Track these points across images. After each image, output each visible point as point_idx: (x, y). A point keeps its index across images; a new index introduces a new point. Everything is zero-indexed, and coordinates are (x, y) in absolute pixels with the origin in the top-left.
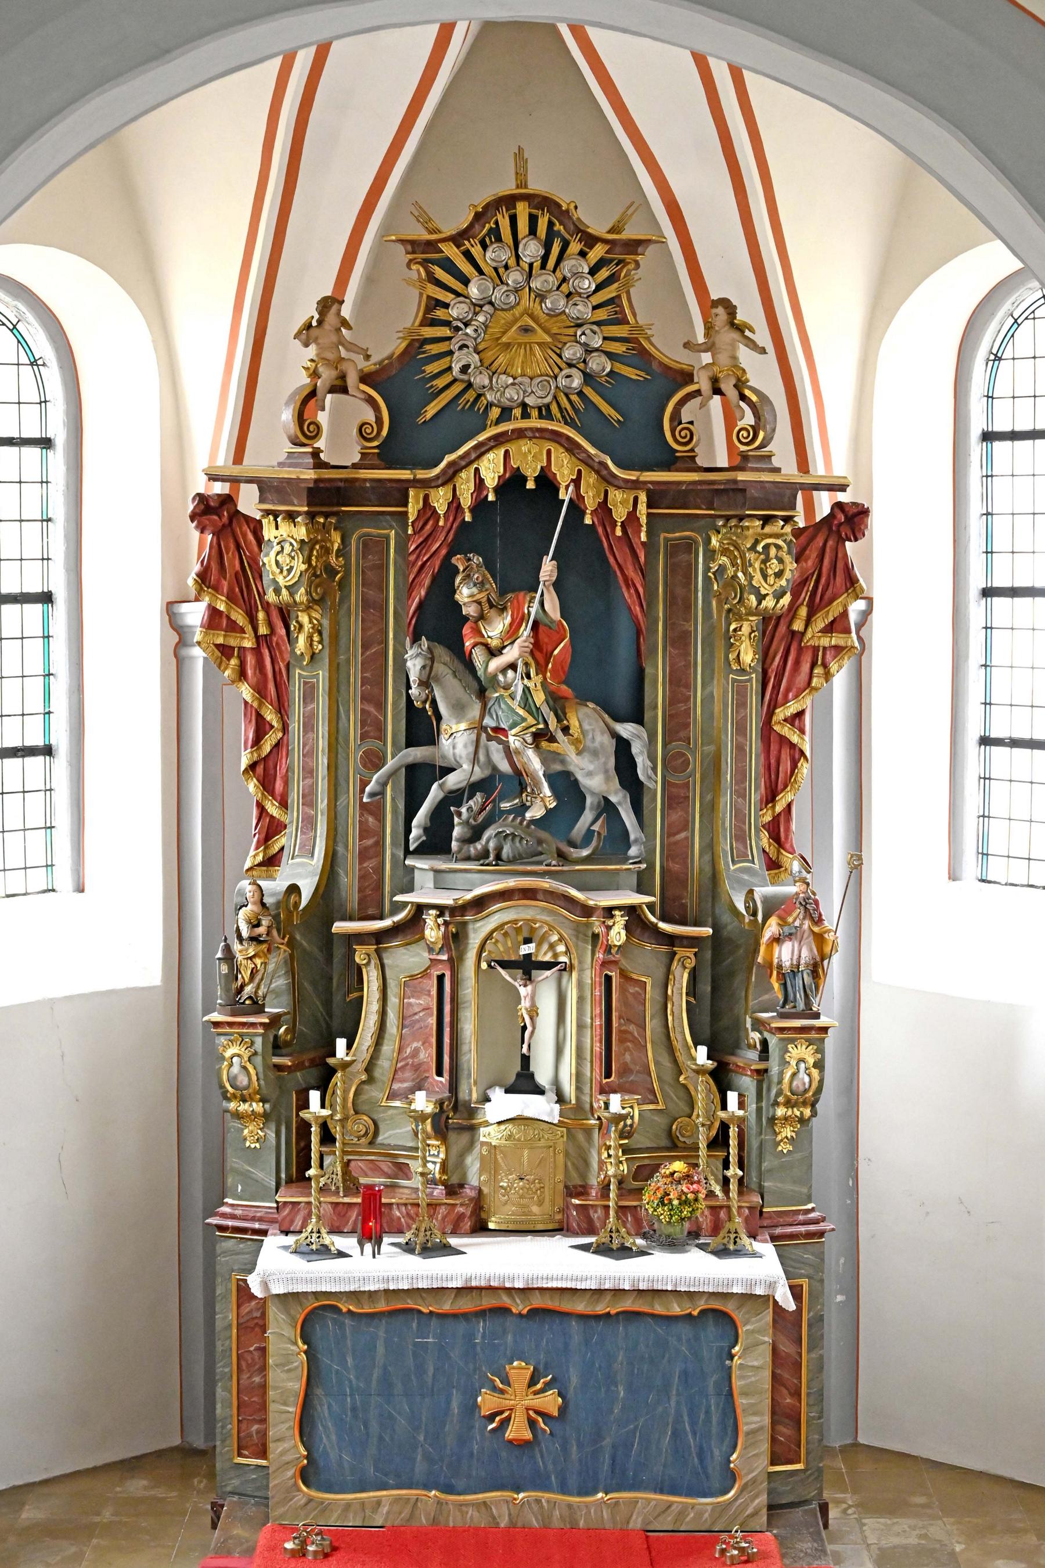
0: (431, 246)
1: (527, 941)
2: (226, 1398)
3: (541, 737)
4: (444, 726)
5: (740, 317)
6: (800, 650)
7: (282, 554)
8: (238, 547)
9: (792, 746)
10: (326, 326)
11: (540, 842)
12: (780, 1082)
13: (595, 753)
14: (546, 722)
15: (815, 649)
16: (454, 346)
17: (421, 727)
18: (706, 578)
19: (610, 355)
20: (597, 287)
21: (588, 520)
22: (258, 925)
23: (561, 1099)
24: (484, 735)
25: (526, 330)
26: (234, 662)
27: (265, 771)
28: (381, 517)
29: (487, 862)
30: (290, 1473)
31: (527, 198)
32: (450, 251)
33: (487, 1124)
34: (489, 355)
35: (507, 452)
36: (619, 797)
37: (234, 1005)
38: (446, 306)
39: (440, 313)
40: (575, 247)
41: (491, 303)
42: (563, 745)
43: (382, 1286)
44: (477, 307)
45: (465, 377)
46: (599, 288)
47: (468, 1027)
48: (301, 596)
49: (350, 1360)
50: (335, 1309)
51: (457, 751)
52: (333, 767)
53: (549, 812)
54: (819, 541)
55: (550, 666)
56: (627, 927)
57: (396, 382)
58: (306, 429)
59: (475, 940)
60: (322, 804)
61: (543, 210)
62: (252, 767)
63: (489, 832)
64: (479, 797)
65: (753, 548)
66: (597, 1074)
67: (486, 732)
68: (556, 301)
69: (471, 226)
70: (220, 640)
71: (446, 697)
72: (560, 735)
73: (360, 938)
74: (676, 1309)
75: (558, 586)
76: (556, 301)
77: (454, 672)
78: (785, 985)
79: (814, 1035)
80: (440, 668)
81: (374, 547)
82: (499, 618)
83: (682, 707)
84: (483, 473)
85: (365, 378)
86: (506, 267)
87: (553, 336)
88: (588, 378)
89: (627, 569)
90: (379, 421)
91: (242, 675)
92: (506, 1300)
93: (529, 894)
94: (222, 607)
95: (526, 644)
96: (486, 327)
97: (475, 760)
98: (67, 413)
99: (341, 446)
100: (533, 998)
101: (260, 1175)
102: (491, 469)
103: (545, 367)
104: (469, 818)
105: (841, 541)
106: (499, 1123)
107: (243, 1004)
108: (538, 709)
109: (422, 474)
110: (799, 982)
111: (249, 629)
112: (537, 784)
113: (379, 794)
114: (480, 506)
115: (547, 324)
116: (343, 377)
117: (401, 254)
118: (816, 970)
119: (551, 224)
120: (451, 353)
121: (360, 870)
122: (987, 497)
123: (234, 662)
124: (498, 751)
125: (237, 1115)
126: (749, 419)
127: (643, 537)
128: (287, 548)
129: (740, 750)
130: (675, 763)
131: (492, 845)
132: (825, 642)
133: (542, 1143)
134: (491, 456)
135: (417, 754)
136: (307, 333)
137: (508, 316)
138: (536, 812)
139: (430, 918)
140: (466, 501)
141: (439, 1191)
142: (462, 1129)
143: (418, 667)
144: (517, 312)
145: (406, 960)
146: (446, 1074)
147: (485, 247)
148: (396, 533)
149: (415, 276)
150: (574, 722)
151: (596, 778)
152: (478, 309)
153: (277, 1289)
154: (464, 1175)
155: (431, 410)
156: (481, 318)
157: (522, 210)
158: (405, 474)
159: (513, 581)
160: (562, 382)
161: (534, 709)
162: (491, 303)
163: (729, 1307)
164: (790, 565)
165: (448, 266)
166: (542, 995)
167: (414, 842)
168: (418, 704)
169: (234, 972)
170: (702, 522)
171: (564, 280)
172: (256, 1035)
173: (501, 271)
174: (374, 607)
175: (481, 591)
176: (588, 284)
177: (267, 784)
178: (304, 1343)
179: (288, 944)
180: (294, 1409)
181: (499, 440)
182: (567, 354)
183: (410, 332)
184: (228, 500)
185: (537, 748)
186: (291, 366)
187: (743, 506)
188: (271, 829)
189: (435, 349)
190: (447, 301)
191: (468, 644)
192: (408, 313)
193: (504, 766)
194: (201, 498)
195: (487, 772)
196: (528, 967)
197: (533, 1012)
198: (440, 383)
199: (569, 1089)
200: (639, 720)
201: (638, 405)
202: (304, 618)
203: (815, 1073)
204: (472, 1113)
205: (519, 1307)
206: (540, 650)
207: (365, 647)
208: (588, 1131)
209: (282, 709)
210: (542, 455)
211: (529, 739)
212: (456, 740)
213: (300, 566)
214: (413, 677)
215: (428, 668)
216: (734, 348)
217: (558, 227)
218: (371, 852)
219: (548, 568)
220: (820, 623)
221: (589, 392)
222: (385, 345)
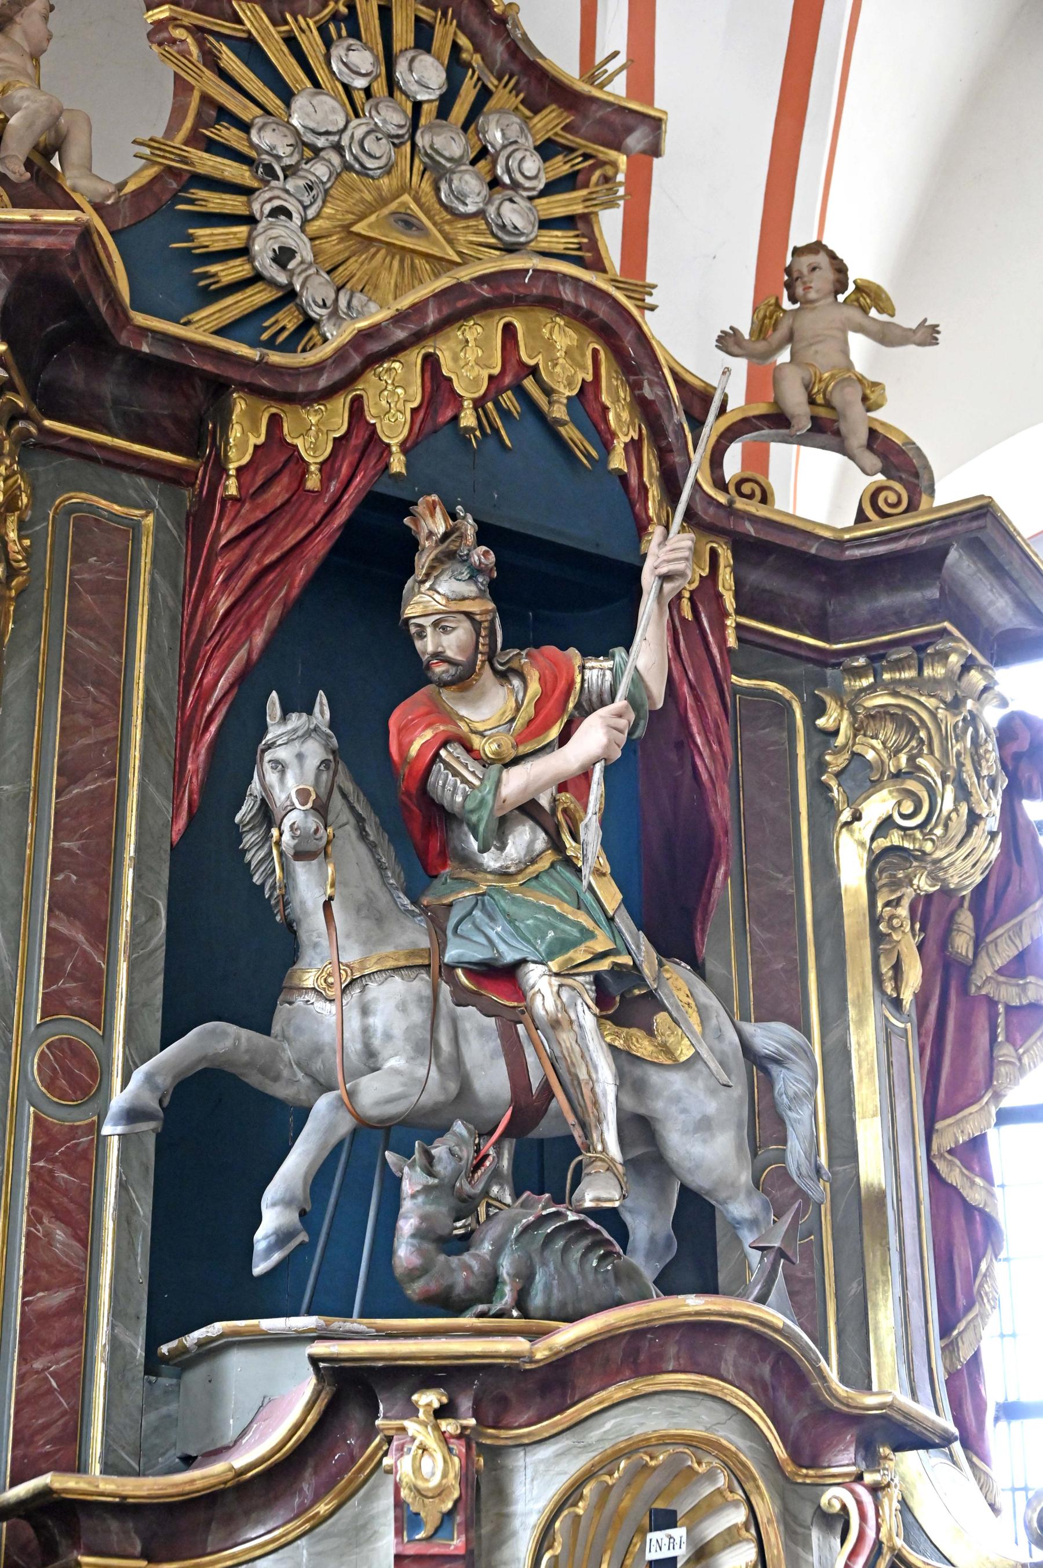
16: (259, 206)
20: (547, 185)
24: (445, 989)
25: (408, 223)
28: (124, 476)
29: (496, 1307)
38: (245, 127)
39: (229, 135)
41: (338, 148)
45: (282, 278)
46: (551, 188)
51: (376, 1021)
61: (444, 14)
67: (453, 981)
89: (707, 697)
96: (326, 191)
108: (610, 920)
115: (447, 228)
121: (21, 1378)
124: (482, 1032)
127: (732, 642)
134: (472, 331)
140: (393, 425)
148: (159, 524)
152: (308, 153)
156: (320, 170)
161: (603, 919)
162: (338, 148)
165: (250, 50)
170: (800, 669)
171: (483, 153)
173: (359, 97)
190: (246, 117)
207: (69, 774)
210: (583, 355)
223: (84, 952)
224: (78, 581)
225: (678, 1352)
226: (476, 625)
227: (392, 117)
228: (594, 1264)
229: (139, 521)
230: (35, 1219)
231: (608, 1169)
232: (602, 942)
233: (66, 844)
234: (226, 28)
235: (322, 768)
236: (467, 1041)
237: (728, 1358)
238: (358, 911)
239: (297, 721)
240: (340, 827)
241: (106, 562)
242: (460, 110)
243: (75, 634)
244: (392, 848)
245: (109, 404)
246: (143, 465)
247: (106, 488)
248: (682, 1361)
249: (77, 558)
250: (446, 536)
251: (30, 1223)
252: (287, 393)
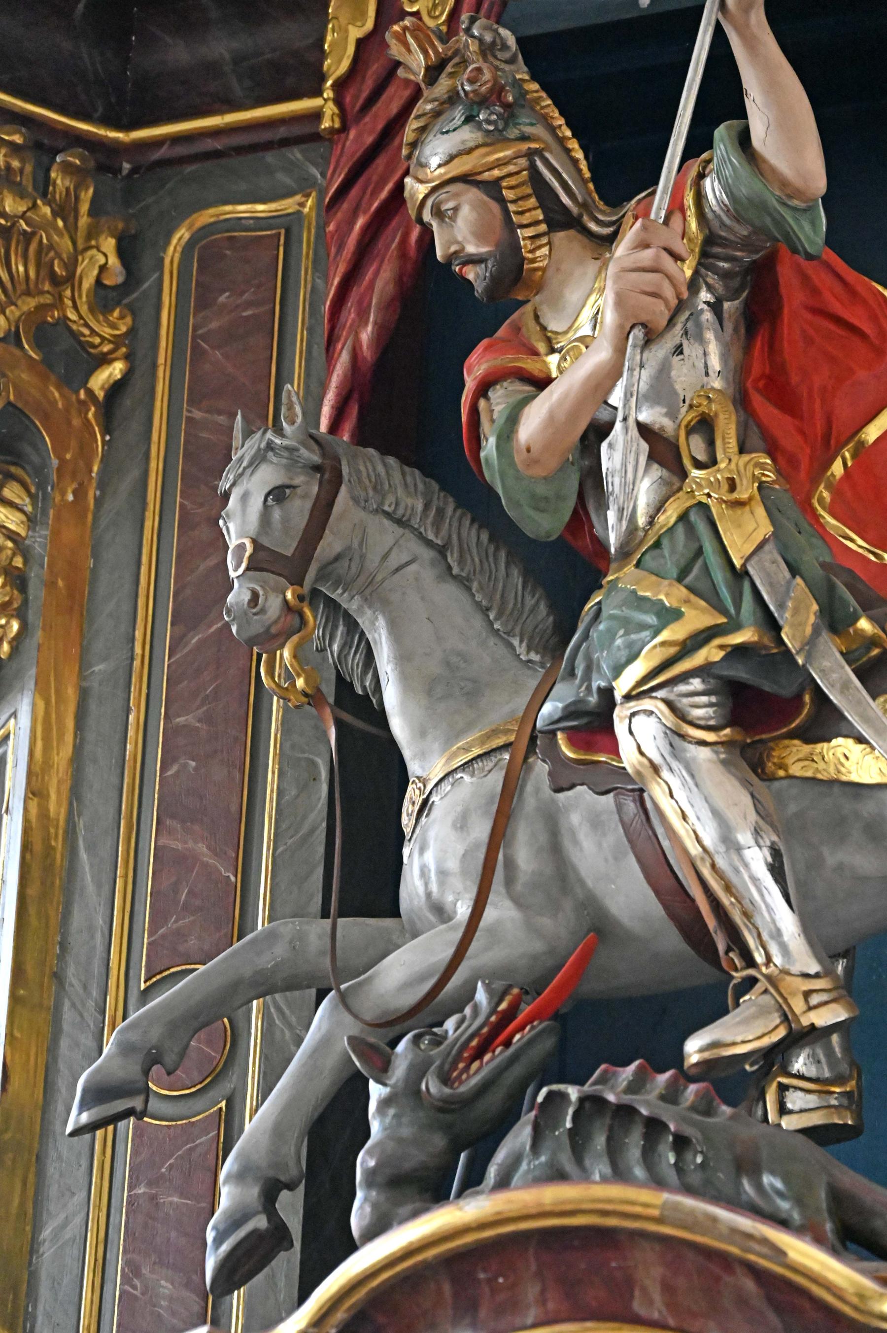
14: (772, 625)
28: (270, 157)
55: (837, 469)
72: (833, 675)
77: (442, 551)
82: (592, 267)
95: (647, 256)
104: (418, 1072)
108: (739, 575)
124: (596, 823)
143: (256, 503)
161: (719, 576)
167: (218, 1242)
175: (496, 138)
193: (629, 896)
195: (558, 926)
211: (702, 710)
215: (299, 510)
223: (206, 865)
224: (203, 337)
225: (543, 1292)
226: (493, 189)
228: (672, 1160)
229: (299, 213)
230: (133, 1270)
231: (766, 991)
232: (697, 617)
233: (181, 720)
235: (270, 502)
236: (576, 842)
237: (647, 1282)
238: (429, 692)
240: (397, 570)
241: (243, 293)
243: (197, 414)
244: (515, 572)
245: (227, 69)
246: (282, 132)
247: (243, 186)
248: (551, 1306)
249: (204, 303)
250: (434, 72)
251: (126, 1279)
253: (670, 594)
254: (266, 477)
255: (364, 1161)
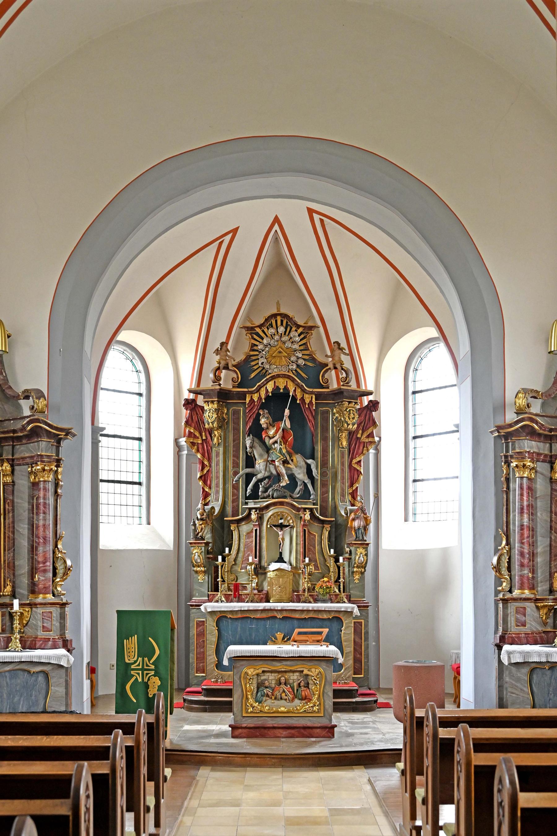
0: (252, 328)
1: (281, 519)
2: (193, 657)
3: (285, 462)
4: (257, 461)
5: (341, 346)
6: (360, 443)
7: (210, 415)
8: (197, 414)
9: (358, 470)
10: (223, 350)
11: (285, 492)
12: (355, 560)
13: (301, 467)
15: (364, 443)
17: (250, 462)
18: (332, 421)
19: (304, 359)
21: (298, 402)
22: (203, 515)
23: (291, 565)
25: (280, 352)
26: (196, 447)
27: (204, 478)
30: (212, 666)
31: (280, 315)
32: (258, 330)
33: (270, 571)
34: (269, 359)
35: (275, 382)
36: (307, 481)
37: (196, 537)
38: (257, 346)
39: (255, 348)
40: (294, 329)
42: (292, 466)
43: (239, 609)
44: (266, 346)
46: (301, 340)
47: (264, 544)
48: (215, 425)
49: (230, 632)
50: (226, 617)
52: (224, 476)
53: (287, 484)
54: (365, 412)
56: (310, 514)
57: (244, 367)
58: (217, 379)
59: (266, 518)
60: (221, 486)
62: (201, 477)
63: (270, 489)
64: (267, 480)
65: (346, 410)
66: (301, 558)
68: (289, 344)
69: (264, 323)
70: (192, 441)
71: (257, 453)
72: (290, 462)
73: (232, 522)
74: (325, 616)
75: (290, 417)
76: (289, 344)
78: (356, 533)
79: (365, 546)
80: (256, 444)
81: (236, 413)
83: (326, 458)
84: (268, 388)
85: (234, 366)
86: (274, 335)
87: (288, 354)
88: (298, 366)
90: (238, 377)
91: (198, 451)
92: (275, 614)
93: (282, 504)
94: (192, 431)
97: (266, 470)
98: (147, 386)
99: (227, 380)
100: (283, 535)
101: (203, 590)
102: (270, 387)
103: (285, 363)
105: (371, 411)
106: (273, 571)
107: (198, 538)
109: (250, 390)
110: (360, 531)
111: (200, 437)
112: (283, 476)
113: (238, 481)
114: (267, 398)
116: (227, 365)
117: (244, 332)
118: (365, 528)
119: (287, 322)
120: (258, 359)
122: (414, 410)
123: (196, 447)
125: (196, 572)
126: (344, 375)
128: (211, 411)
129: (343, 470)
130: (323, 474)
131: (271, 493)
132: (367, 440)
133: (286, 577)
134: (270, 383)
135: (249, 470)
136: (217, 352)
137: (275, 349)
138: (283, 484)
139: (253, 512)
140: (263, 396)
141: (256, 592)
142: (262, 574)
144: (277, 347)
145: (245, 528)
146: (258, 558)
147: (268, 329)
149: (248, 337)
150: (294, 459)
151: (301, 475)
153: (209, 610)
154: (263, 588)
155: (253, 375)
156: (267, 349)
157: (279, 319)
158: (246, 390)
159: (277, 418)
160: (291, 367)
163: (341, 616)
164: (357, 416)
166: (285, 536)
168: (249, 454)
169: (195, 530)
170: (331, 405)
171: (291, 338)
172: (202, 546)
174: (236, 430)
176: (298, 339)
177: (205, 482)
178: (217, 626)
179: (211, 523)
180: (214, 647)
181: (273, 378)
182: (292, 359)
183: (246, 353)
184: (194, 401)
185: (284, 466)
186: (213, 360)
187: (343, 398)
188: (206, 495)
189: (254, 358)
191: (263, 436)
192: (246, 348)
193: (274, 472)
194: (186, 400)
196: (282, 526)
197: (283, 539)
198: (255, 367)
199: (294, 562)
200: (313, 459)
201: (313, 372)
202: (216, 433)
203: (365, 557)
204: (265, 569)
205: (279, 616)
206: (284, 438)
207: (234, 441)
208: (299, 575)
209: (209, 460)
212: (260, 464)
213: (215, 416)
214: (248, 446)
216: (340, 355)
217: (289, 323)
218: (235, 500)
219: (287, 412)
220: (365, 435)
221: (298, 370)
222: (240, 357)
227: (277, 337)
234: (254, 332)
239: (249, 438)
242: (287, 333)
252: (252, 393)
253: (279, 455)
254: (250, 441)
255: (260, 490)
